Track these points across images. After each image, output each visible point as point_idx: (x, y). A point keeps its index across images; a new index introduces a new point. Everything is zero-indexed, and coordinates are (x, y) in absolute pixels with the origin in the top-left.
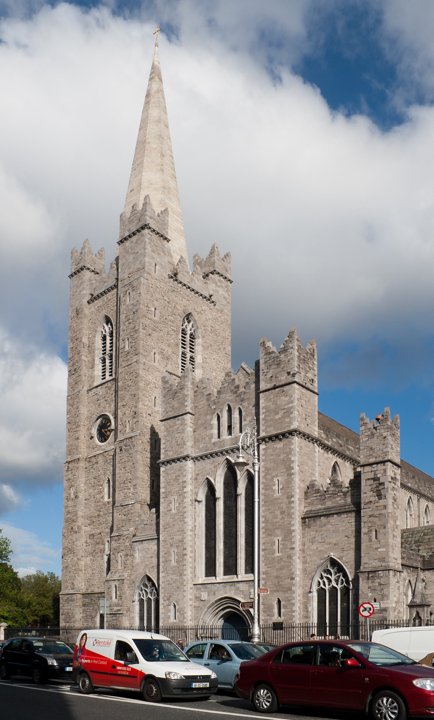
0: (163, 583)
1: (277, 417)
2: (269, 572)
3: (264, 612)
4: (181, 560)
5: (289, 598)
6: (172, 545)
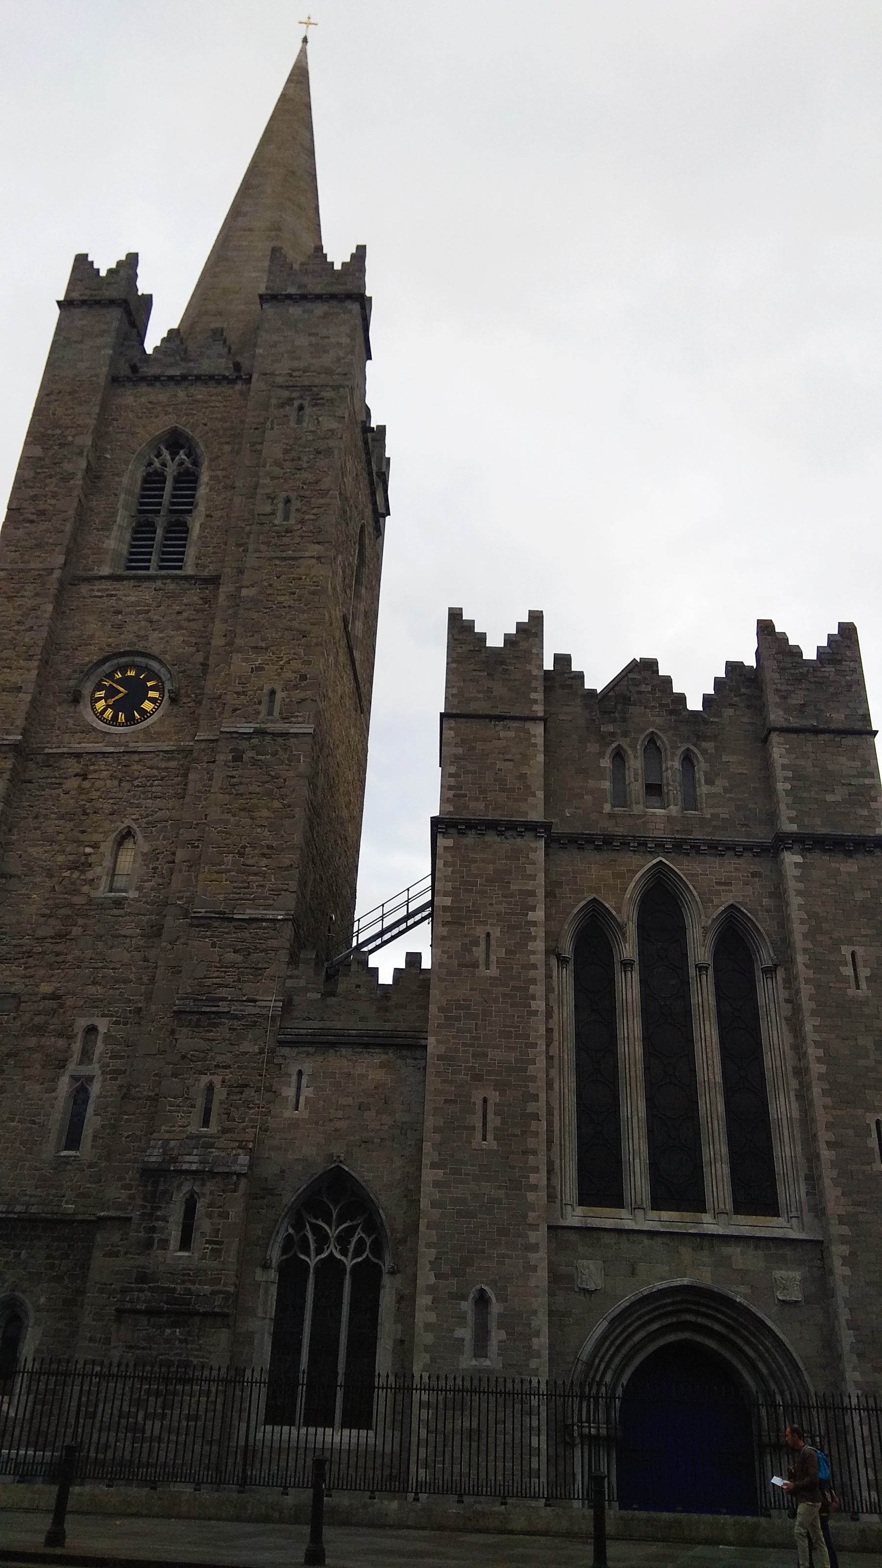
0: (434, 1204)
1: (830, 798)
6: (477, 1078)
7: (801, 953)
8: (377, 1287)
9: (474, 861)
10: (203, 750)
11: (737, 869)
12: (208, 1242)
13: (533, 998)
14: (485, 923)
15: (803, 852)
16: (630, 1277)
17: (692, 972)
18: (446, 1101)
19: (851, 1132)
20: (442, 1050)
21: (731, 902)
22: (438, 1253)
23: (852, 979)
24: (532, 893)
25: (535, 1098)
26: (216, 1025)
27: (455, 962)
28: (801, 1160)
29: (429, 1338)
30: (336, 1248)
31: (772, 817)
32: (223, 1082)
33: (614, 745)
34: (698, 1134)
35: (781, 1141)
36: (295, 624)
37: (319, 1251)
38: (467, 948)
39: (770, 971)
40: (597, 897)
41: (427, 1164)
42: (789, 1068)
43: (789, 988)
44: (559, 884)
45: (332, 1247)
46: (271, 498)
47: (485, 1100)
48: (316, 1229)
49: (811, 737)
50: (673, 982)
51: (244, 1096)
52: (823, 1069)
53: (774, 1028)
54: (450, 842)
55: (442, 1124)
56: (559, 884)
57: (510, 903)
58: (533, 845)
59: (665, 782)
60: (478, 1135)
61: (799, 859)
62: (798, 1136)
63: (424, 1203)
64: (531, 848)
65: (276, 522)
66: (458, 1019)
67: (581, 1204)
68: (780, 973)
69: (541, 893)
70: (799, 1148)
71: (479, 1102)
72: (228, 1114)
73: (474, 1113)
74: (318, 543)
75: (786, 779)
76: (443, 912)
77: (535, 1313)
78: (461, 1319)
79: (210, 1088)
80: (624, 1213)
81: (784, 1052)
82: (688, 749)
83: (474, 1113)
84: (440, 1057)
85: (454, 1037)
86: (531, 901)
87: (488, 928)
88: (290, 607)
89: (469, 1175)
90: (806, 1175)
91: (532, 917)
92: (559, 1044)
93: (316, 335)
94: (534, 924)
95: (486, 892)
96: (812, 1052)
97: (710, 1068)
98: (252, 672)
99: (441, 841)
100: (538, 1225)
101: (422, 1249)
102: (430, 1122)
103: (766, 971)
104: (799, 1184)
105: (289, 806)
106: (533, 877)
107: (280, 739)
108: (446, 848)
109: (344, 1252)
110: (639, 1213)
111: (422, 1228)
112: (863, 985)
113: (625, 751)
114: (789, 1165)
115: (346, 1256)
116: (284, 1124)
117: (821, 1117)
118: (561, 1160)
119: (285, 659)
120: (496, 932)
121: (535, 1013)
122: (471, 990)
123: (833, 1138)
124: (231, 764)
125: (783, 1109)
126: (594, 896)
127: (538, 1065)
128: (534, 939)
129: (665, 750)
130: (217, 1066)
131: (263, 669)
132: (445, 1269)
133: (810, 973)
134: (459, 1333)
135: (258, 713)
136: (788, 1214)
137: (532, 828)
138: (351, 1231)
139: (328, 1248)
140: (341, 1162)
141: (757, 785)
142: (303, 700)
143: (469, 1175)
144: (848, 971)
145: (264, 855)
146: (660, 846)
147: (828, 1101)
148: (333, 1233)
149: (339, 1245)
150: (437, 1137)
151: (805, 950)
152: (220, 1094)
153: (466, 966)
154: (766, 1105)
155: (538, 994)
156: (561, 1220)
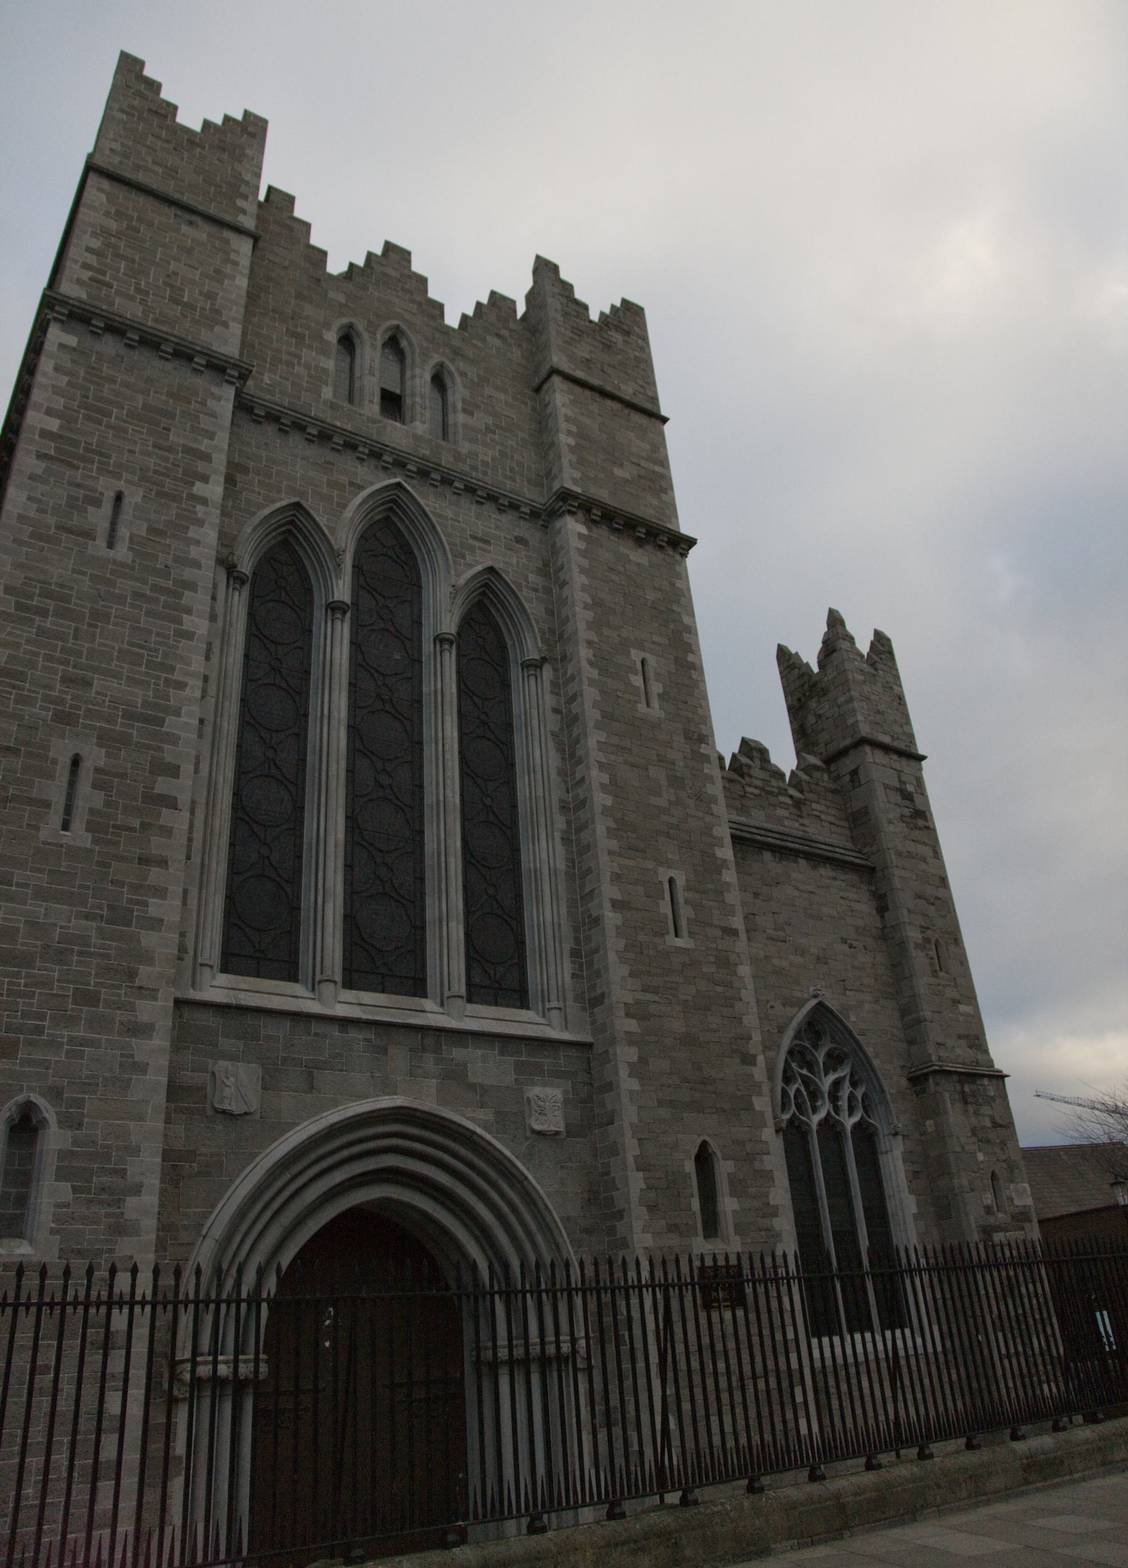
1: (618, 472)
2: (652, 1008)
3: (652, 1208)
4: (136, 823)
5: (749, 1147)
6: (65, 718)
7: (585, 644)
11: (497, 527)
13: (189, 611)
14: (117, 476)
15: (591, 522)
16: (306, 1092)
17: (428, 646)
19: (640, 890)
21: (490, 564)
24: (207, 458)
25: (173, 771)
27: (52, 520)
28: (566, 928)
31: (549, 475)
40: (303, 502)
42: (555, 799)
43: (558, 694)
44: (245, 470)
47: (76, 762)
49: (597, 397)
50: (397, 656)
52: (609, 801)
53: (537, 744)
54: (72, 340)
56: (245, 470)
57: (166, 460)
58: (215, 390)
60: (55, 818)
61: (583, 529)
62: (563, 893)
64: (212, 394)
66: (43, 613)
67: (225, 969)
68: (547, 673)
69: (220, 461)
70: (564, 910)
71: (65, 761)
75: (569, 433)
80: (298, 989)
81: (549, 778)
86: (201, 466)
87: (121, 485)
89: (26, 886)
91: (199, 488)
92: (217, 702)
94: (204, 501)
96: (597, 777)
97: (448, 782)
99: (55, 335)
100: (157, 990)
104: (562, 964)
106: (211, 435)
108: (62, 346)
110: (327, 989)
112: (655, 703)
114: (549, 932)
117: (606, 864)
118: (200, 890)
120: (134, 498)
121: (190, 636)
122: (74, 571)
123: (618, 897)
125: (544, 855)
127: (183, 719)
128: (200, 523)
133: (594, 673)
136: (543, 1002)
137: (217, 367)
143: (26, 886)
144: (637, 681)
146: (400, 464)
147: (614, 844)
151: (589, 643)
154: (515, 851)
156: (191, 991)
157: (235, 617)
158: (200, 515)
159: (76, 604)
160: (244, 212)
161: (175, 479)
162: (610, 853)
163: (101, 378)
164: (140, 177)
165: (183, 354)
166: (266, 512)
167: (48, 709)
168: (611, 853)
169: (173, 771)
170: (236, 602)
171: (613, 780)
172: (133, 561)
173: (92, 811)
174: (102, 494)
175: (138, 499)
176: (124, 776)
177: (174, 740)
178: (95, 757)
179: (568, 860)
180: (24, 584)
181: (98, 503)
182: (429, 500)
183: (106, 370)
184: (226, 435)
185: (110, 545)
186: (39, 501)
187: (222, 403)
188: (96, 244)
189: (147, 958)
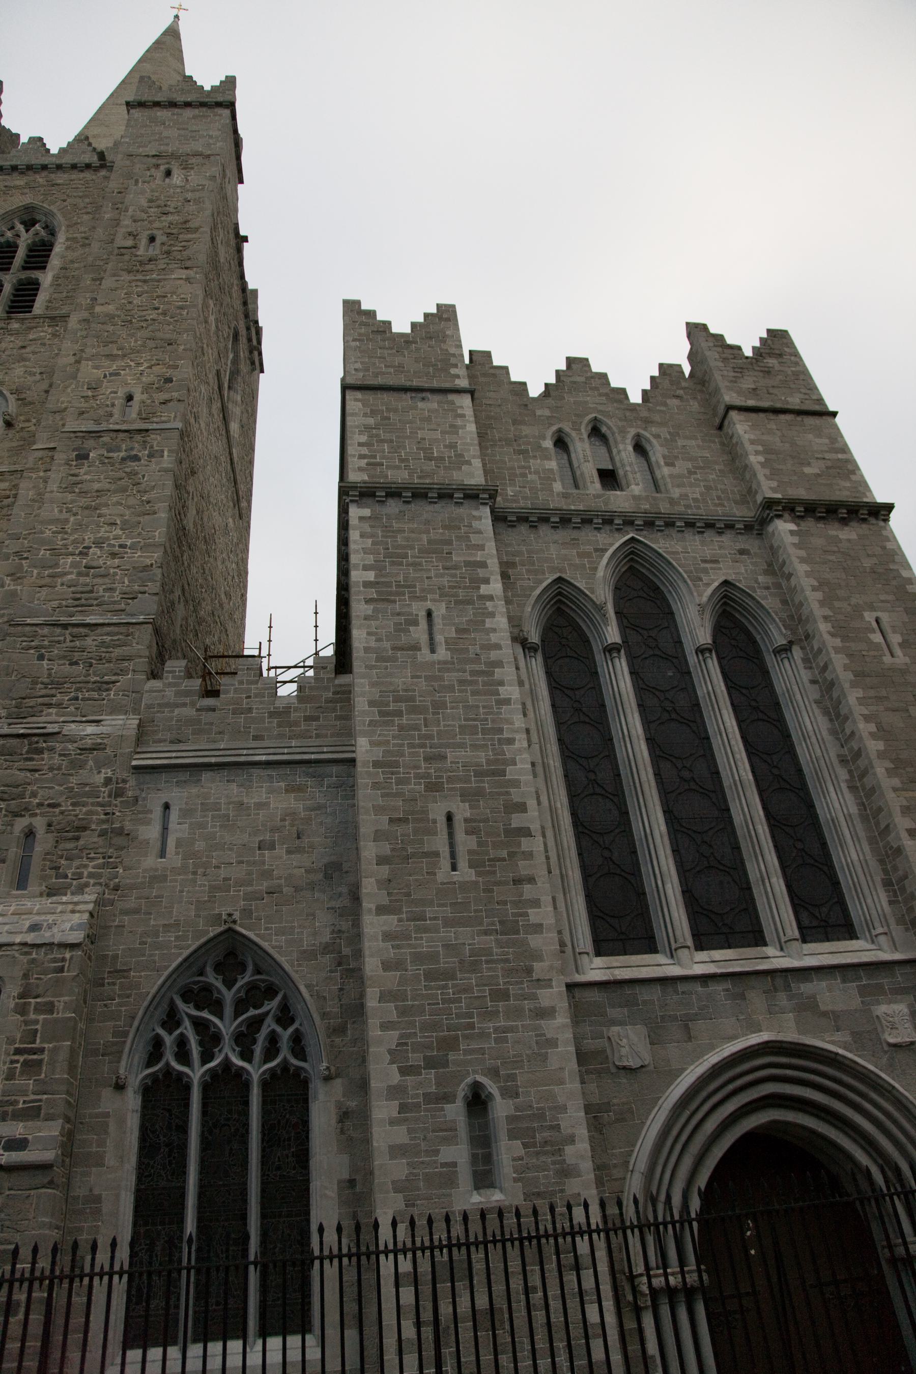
0: (387, 966)
1: (807, 470)
6: (434, 787)
7: (822, 620)
8: (303, 1102)
9: (401, 531)
10: (41, 459)
11: (721, 547)
12: (18, 1052)
13: (501, 683)
15: (798, 518)
16: (686, 1042)
17: (692, 659)
18: (391, 820)
20: (378, 753)
22: (402, 1036)
23: (885, 647)
24: (483, 565)
26: (40, 751)
27: (387, 645)
28: (873, 863)
29: (399, 1169)
30: (234, 1050)
31: (751, 492)
32: (49, 825)
33: (554, 428)
34: (737, 848)
35: (843, 844)
36: (159, 335)
37: (206, 1057)
38: (400, 629)
39: (785, 650)
40: (564, 576)
41: (370, 910)
42: (833, 755)
43: (811, 668)
44: (513, 565)
45: (227, 1050)
46: (133, 235)
47: (449, 818)
48: (200, 1025)
49: (772, 416)
50: (670, 674)
51: (81, 842)
52: (880, 745)
54: (367, 512)
55: (389, 852)
56: (513, 565)
57: (455, 576)
58: (475, 513)
59: (618, 464)
60: (445, 863)
61: (792, 527)
62: (862, 834)
63: (371, 965)
65: (138, 253)
66: (399, 713)
67: (598, 954)
68: (797, 652)
69: (493, 564)
70: (866, 848)
72: (57, 868)
73: (435, 834)
74: (186, 268)
75: (757, 453)
76: (364, 587)
77: (564, 1109)
78: (448, 1133)
79: (30, 834)
80: (660, 958)
81: (823, 739)
82: (638, 435)
83: (435, 834)
84: (376, 764)
85: (394, 737)
86: (481, 573)
87: (429, 605)
88: (154, 320)
89: (435, 918)
90: (883, 880)
91: (484, 589)
93: (187, 129)
94: (491, 598)
95: (420, 564)
96: (864, 728)
97: (739, 764)
98: (105, 376)
99: (355, 512)
100: (551, 980)
101: (374, 1031)
102: (369, 850)
103: (778, 651)
104: (878, 894)
105: (148, 502)
106: (481, 547)
107: (138, 437)
108: (361, 519)
109: (247, 1056)
110: (683, 954)
111: (372, 1003)
112: (898, 652)
113: (567, 435)
115: (249, 1061)
116: (144, 877)
117: (894, 801)
118: (565, 894)
119: (146, 365)
120: (440, 610)
121: (507, 702)
124: (74, 463)
125: (837, 805)
126: (558, 575)
127: (519, 766)
128: (492, 615)
129: (613, 434)
130: (40, 805)
131: (118, 374)
132: (415, 1058)
133: (838, 642)
134: (449, 1153)
135: (111, 415)
136: (869, 931)
137: (472, 495)
138: (256, 1023)
139: (220, 1051)
140: (234, 922)
141: (722, 467)
142: (170, 401)
143: (435, 918)
144: (877, 638)
145: (114, 555)
146: (629, 522)
147: (896, 782)
148: (226, 1027)
149: (238, 1046)
150: (385, 871)
151: (826, 618)
152: (43, 843)
153: (402, 649)
154: (811, 806)
155: (507, 679)
156: (577, 975)
157: (536, 677)
158: (490, 609)
159: (420, 701)
160: (458, 377)
161: (465, 587)
162: (895, 790)
163: (393, 532)
164: (380, 381)
165: (445, 495)
166: (538, 592)
167: (420, 784)
168: (895, 790)
169: (522, 808)
170: (534, 667)
171: (879, 727)
172: (452, 658)
173: (470, 852)
174: (417, 615)
175: (443, 611)
176: (486, 820)
177: (516, 783)
178: (462, 811)
179: (858, 804)
180: (380, 696)
181: (415, 623)
182: (660, 543)
183: (395, 525)
184: (493, 544)
185: (433, 651)
186: (376, 634)
187: (483, 521)
188: (363, 439)
189: (537, 956)
